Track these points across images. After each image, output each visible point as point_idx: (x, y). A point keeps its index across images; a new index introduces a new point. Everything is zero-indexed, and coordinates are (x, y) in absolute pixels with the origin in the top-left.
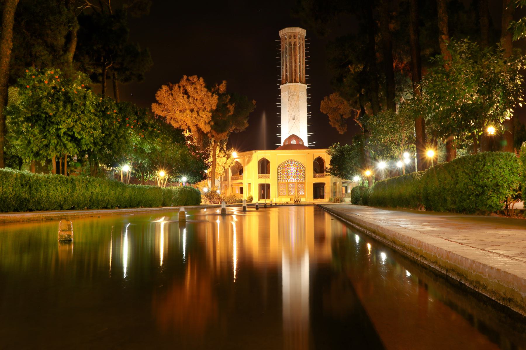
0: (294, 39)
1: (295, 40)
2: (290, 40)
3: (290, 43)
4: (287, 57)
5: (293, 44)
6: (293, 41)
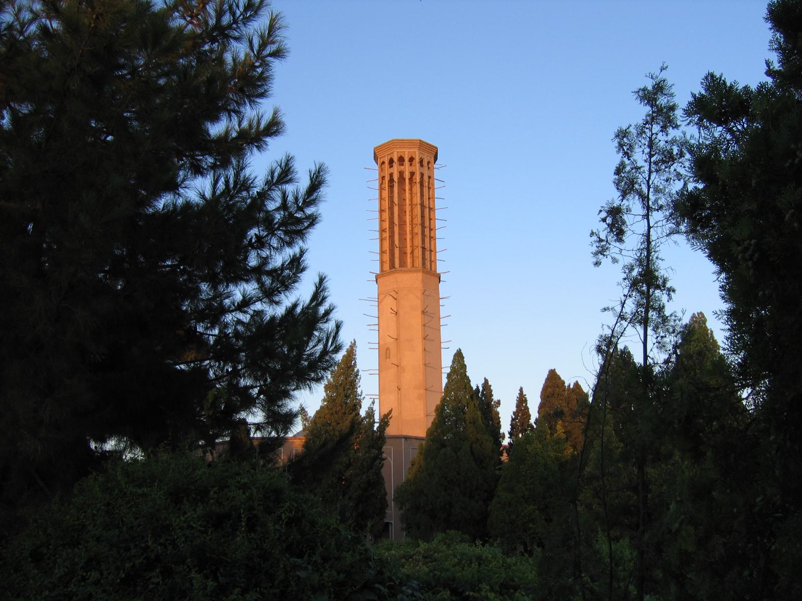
1: (413, 169)
3: (401, 174)
5: (407, 176)
6: (407, 169)
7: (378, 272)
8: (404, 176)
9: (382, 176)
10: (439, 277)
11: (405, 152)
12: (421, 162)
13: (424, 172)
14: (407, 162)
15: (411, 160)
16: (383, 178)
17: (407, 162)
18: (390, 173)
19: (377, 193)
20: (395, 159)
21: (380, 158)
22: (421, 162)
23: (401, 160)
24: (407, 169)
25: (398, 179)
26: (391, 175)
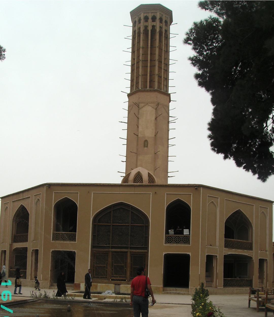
0: (153, 21)
1: (154, 24)
2: (146, 24)
3: (146, 27)
4: (140, 49)
5: (150, 28)
7: (129, 92)
8: (148, 29)
9: (134, 30)
10: (169, 95)
11: (149, 13)
12: (161, 20)
13: (162, 26)
14: (150, 20)
15: (154, 19)
16: (134, 32)
17: (150, 20)
18: (139, 27)
19: (130, 42)
20: (142, 18)
21: (134, 19)
22: (161, 20)
23: (146, 19)
24: (150, 24)
25: (143, 30)
26: (139, 29)
